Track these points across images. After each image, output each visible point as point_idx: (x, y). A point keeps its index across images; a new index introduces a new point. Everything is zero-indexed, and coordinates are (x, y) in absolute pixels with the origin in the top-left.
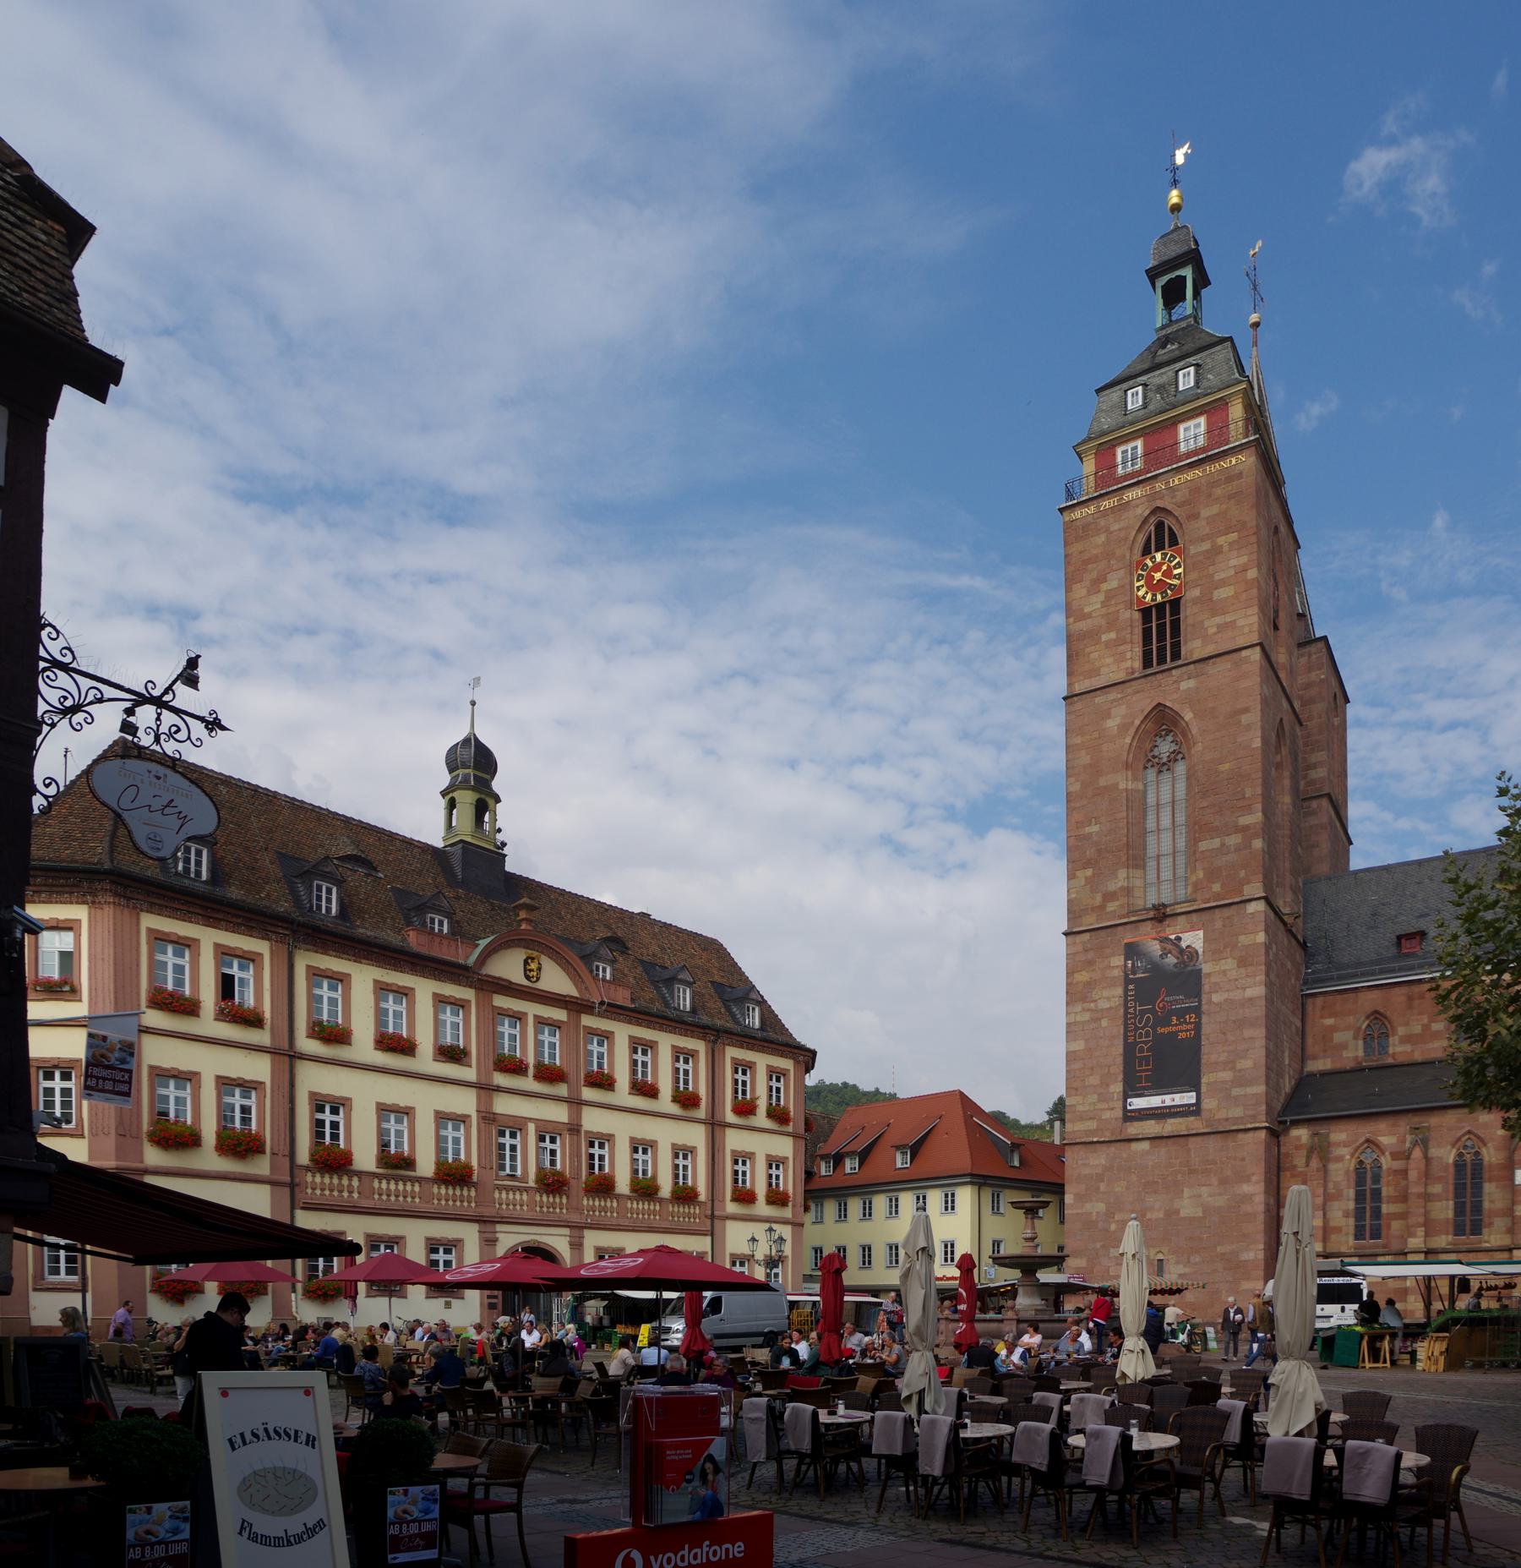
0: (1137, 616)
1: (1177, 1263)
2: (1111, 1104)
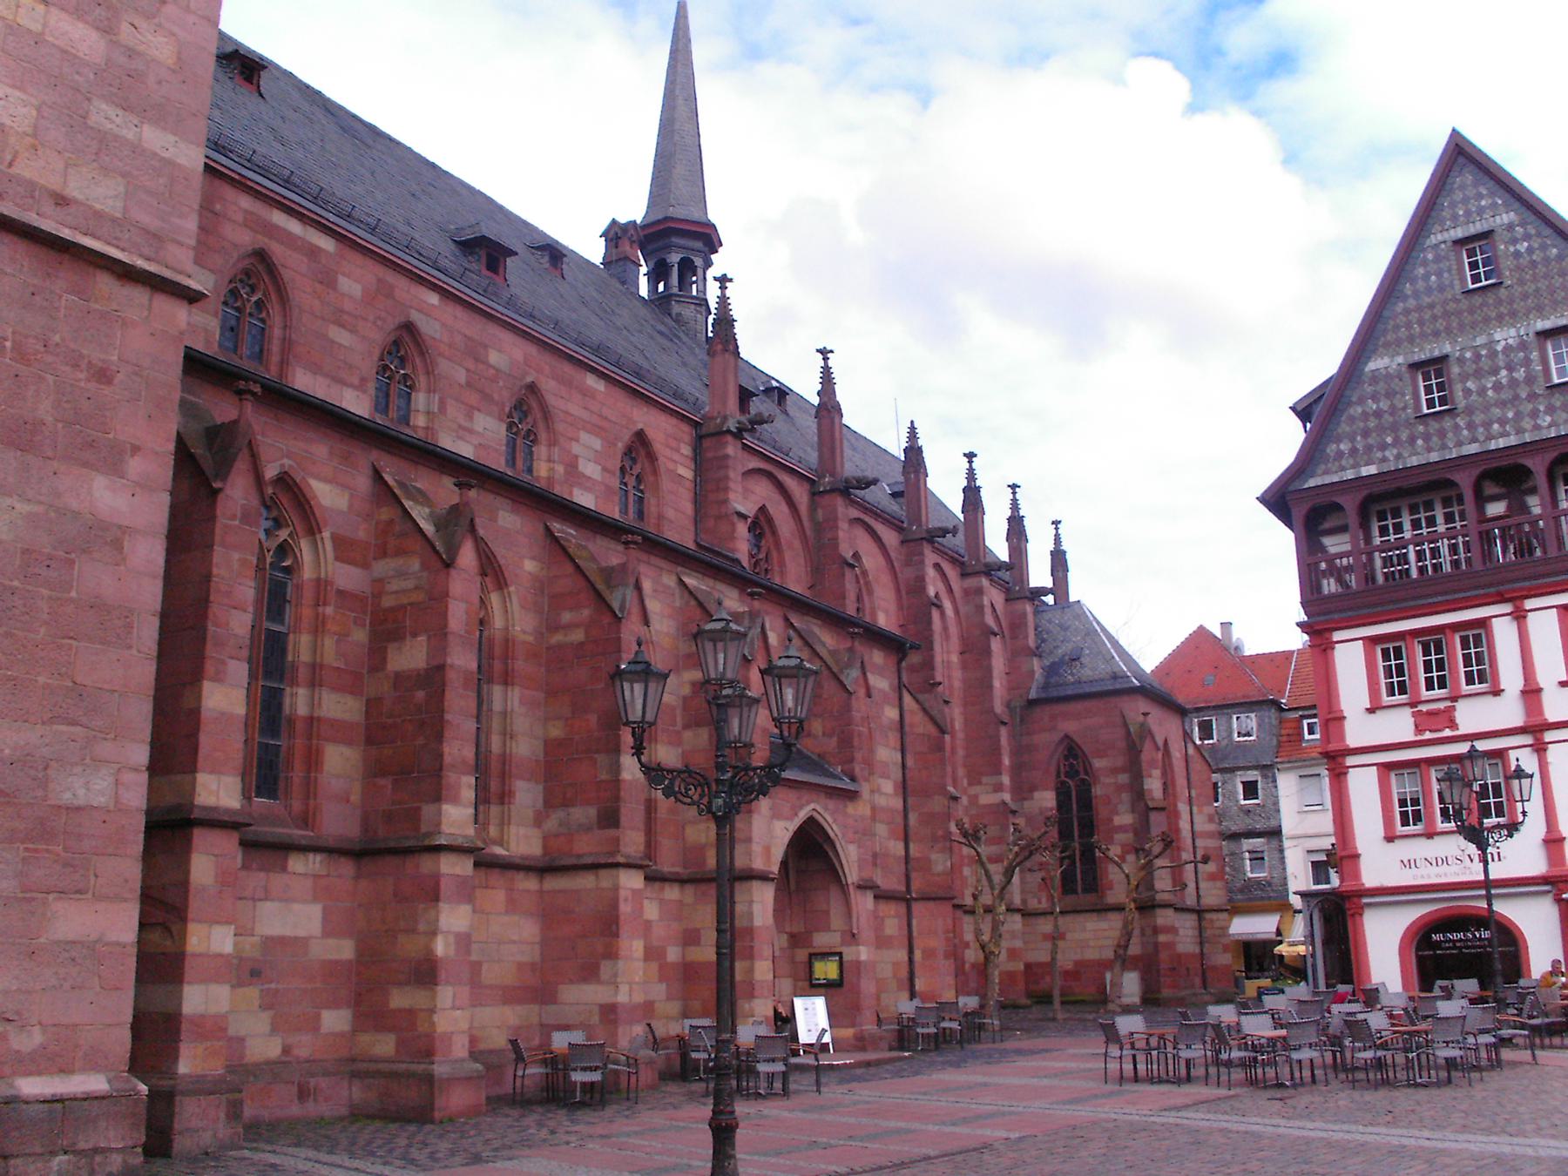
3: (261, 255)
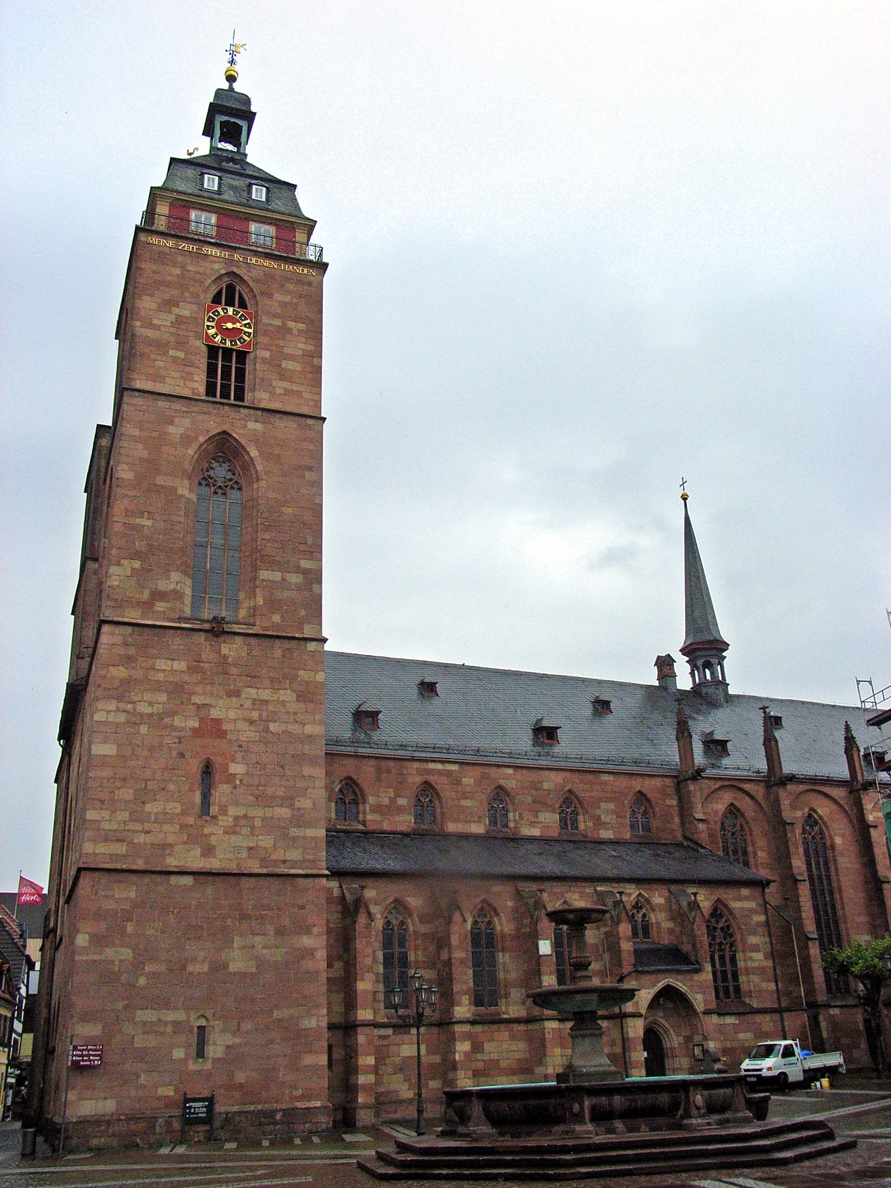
0: (204, 349)
1: (224, 1031)
2: (147, 826)
3: (427, 783)
